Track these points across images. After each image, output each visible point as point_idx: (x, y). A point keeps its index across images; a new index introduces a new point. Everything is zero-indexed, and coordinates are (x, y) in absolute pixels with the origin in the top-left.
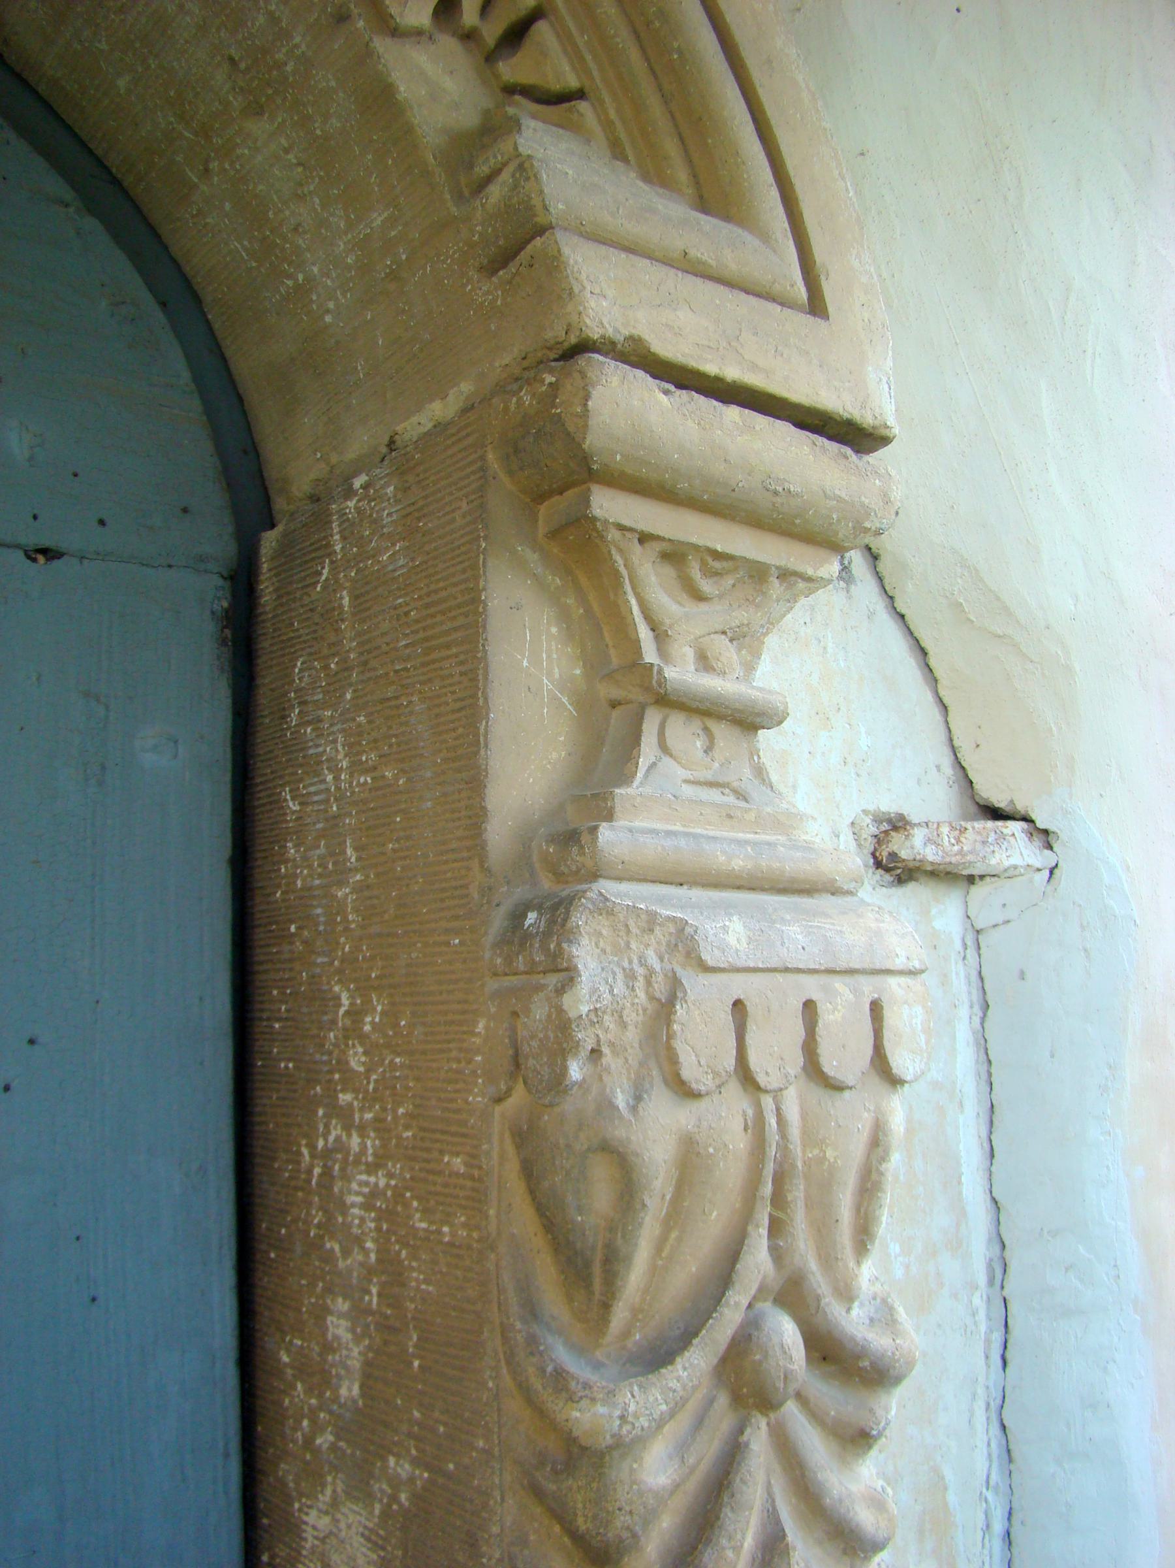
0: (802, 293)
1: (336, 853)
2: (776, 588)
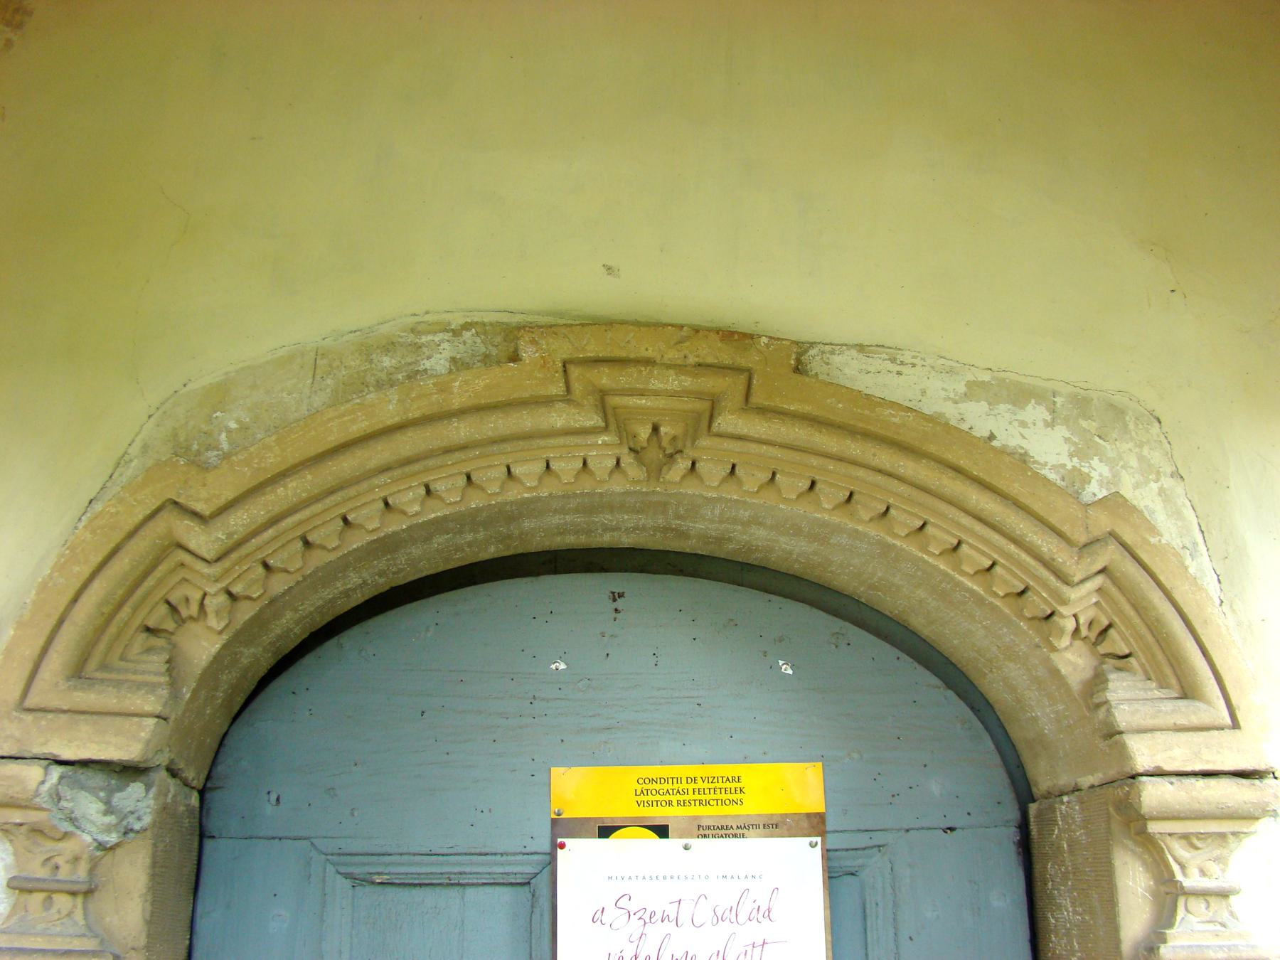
0: (1228, 721)
1: (1070, 942)
2: (1231, 839)
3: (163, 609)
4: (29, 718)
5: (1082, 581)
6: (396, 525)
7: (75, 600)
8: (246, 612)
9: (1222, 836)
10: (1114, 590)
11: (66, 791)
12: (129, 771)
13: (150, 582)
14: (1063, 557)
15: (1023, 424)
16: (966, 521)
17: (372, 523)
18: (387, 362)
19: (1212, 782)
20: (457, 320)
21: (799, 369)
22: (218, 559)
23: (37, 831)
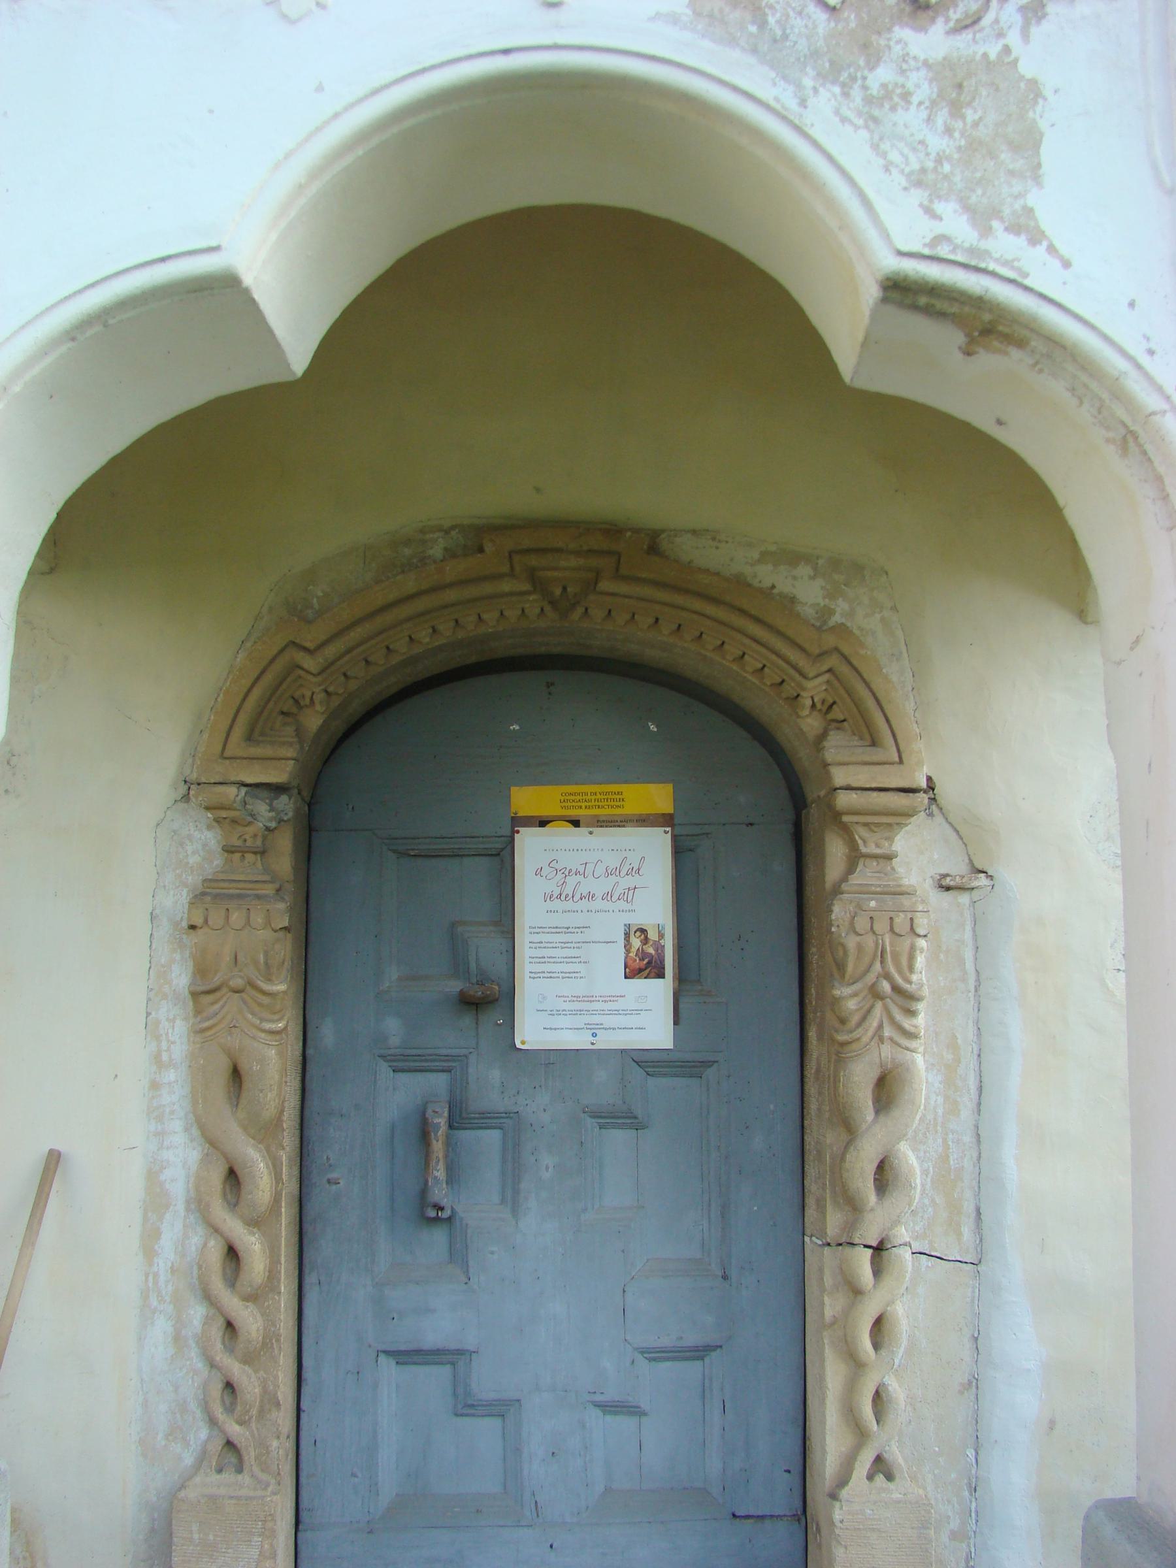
0: (897, 759)
2: (895, 827)
3: (291, 701)
5: (816, 677)
6: (417, 650)
7: (244, 699)
8: (336, 702)
9: (890, 825)
10: (835, 682)
11: (248, 799)
12: (278, 789)
13: (284, 686)
14: (802, 663)
15: (795, 578)
16: (747, 641)
17: (402, 648)
18: (407, 551)
19: (882, 794)
20: (447, 524)
21: (653, 549)
22: (319, 674)
23: (234, 821)
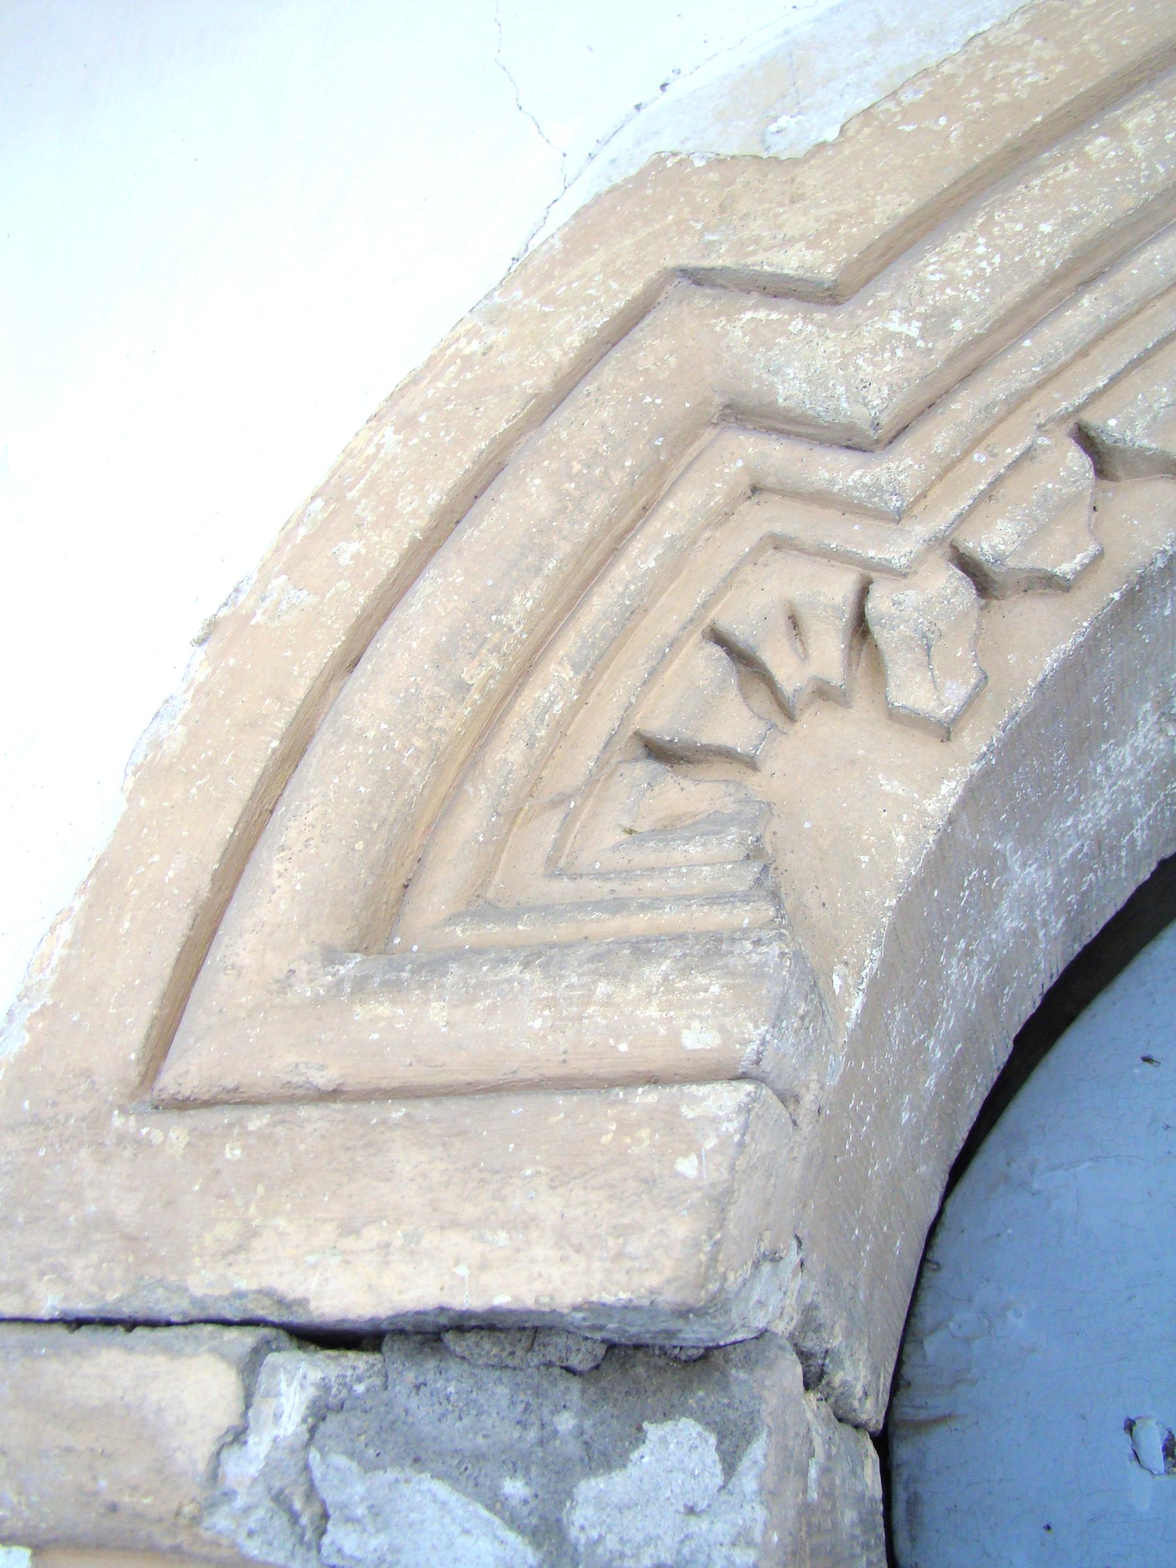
3: (708, 663)
4: (175, 1134)
7: (350, 660)
8: (1041, 640)
11: (343, 1479)
12: (638, 1363)
13: (642, 558)
